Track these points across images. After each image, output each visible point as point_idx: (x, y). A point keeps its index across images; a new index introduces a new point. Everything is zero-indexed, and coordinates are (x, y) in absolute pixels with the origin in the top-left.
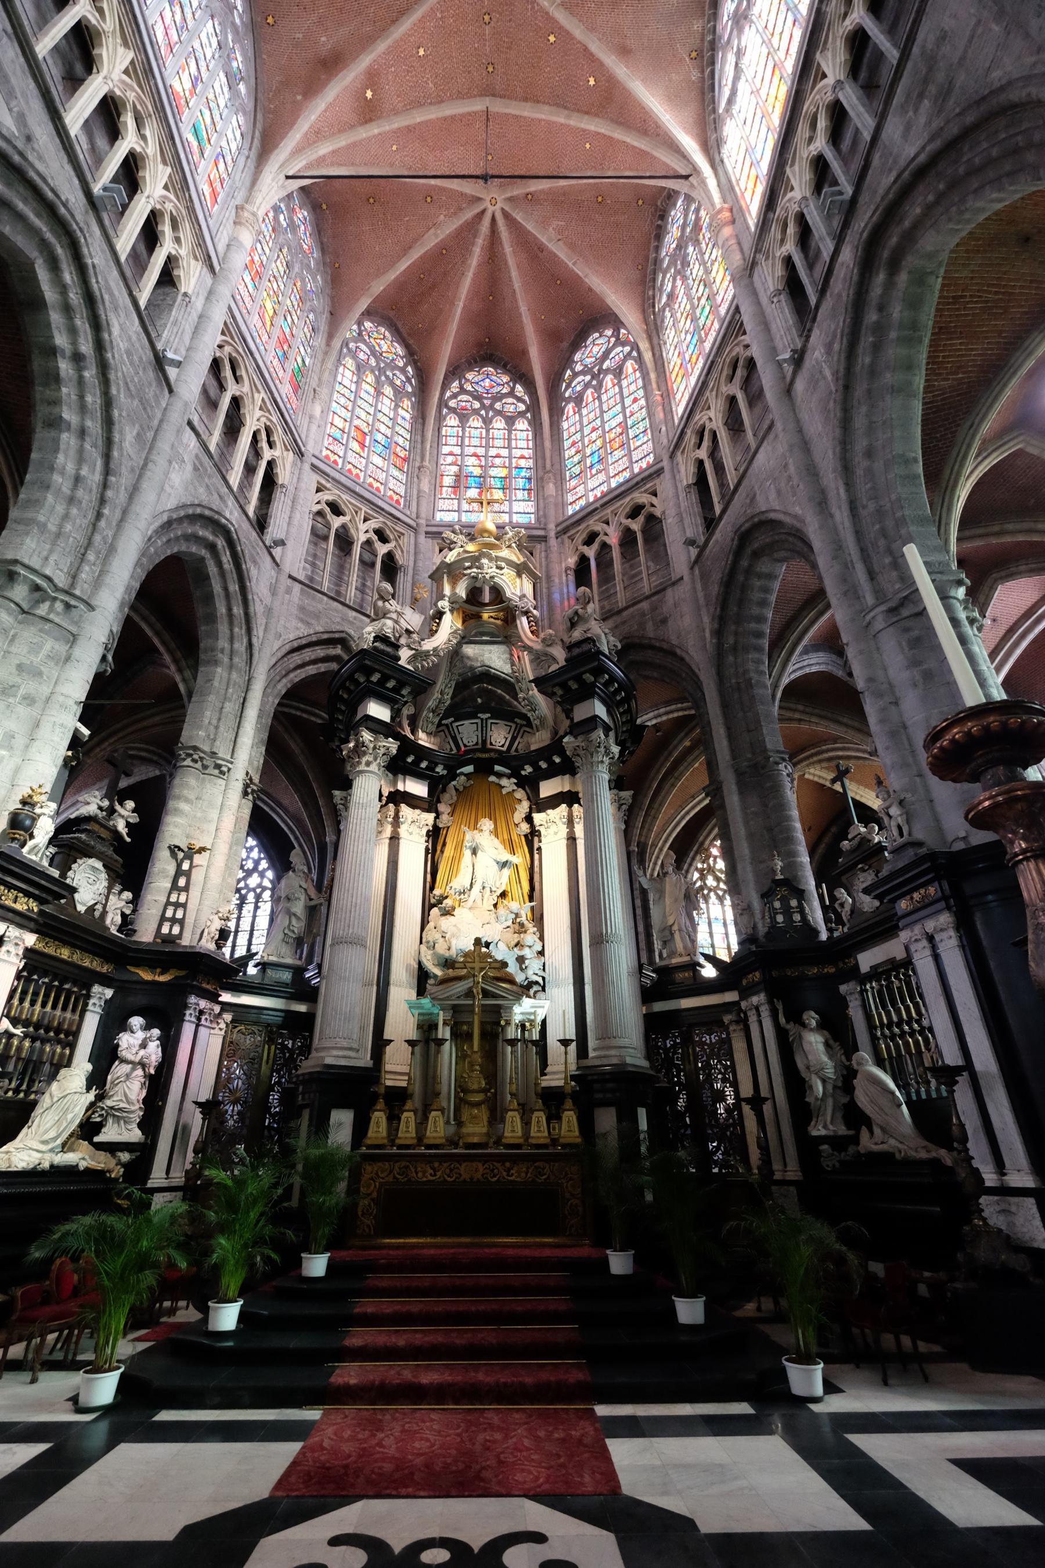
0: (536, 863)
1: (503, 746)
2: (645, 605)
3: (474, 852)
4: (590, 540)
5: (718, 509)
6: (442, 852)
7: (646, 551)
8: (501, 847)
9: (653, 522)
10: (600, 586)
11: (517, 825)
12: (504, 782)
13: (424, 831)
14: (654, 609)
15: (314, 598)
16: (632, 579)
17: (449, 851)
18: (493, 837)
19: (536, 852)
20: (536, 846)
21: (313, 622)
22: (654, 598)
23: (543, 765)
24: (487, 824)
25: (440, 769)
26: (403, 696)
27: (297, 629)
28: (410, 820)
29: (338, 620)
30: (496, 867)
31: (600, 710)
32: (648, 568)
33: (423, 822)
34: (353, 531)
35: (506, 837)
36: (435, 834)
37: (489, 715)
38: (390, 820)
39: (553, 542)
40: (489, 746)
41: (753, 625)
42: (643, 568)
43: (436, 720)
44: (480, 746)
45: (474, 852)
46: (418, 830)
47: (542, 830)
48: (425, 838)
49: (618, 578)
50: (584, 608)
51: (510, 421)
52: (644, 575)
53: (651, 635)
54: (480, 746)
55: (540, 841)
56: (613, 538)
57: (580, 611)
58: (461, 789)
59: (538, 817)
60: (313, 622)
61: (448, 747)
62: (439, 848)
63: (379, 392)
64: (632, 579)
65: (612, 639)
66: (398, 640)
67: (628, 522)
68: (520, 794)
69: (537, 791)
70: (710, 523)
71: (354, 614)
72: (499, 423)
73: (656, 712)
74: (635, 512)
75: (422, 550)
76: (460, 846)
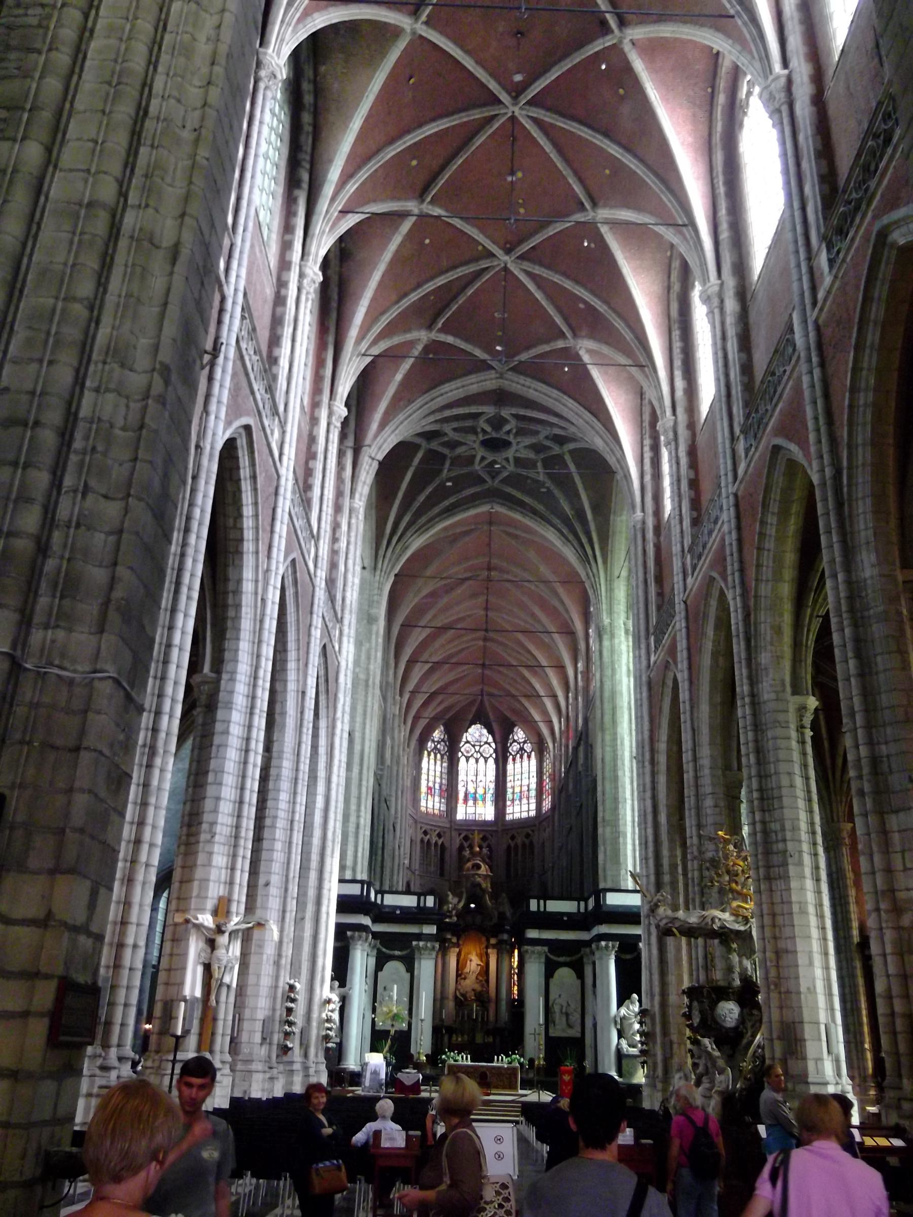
9: (531, 843)
36: (459, 955)
51: (486, 759)
72: (482, 760)
74: (528, 836)
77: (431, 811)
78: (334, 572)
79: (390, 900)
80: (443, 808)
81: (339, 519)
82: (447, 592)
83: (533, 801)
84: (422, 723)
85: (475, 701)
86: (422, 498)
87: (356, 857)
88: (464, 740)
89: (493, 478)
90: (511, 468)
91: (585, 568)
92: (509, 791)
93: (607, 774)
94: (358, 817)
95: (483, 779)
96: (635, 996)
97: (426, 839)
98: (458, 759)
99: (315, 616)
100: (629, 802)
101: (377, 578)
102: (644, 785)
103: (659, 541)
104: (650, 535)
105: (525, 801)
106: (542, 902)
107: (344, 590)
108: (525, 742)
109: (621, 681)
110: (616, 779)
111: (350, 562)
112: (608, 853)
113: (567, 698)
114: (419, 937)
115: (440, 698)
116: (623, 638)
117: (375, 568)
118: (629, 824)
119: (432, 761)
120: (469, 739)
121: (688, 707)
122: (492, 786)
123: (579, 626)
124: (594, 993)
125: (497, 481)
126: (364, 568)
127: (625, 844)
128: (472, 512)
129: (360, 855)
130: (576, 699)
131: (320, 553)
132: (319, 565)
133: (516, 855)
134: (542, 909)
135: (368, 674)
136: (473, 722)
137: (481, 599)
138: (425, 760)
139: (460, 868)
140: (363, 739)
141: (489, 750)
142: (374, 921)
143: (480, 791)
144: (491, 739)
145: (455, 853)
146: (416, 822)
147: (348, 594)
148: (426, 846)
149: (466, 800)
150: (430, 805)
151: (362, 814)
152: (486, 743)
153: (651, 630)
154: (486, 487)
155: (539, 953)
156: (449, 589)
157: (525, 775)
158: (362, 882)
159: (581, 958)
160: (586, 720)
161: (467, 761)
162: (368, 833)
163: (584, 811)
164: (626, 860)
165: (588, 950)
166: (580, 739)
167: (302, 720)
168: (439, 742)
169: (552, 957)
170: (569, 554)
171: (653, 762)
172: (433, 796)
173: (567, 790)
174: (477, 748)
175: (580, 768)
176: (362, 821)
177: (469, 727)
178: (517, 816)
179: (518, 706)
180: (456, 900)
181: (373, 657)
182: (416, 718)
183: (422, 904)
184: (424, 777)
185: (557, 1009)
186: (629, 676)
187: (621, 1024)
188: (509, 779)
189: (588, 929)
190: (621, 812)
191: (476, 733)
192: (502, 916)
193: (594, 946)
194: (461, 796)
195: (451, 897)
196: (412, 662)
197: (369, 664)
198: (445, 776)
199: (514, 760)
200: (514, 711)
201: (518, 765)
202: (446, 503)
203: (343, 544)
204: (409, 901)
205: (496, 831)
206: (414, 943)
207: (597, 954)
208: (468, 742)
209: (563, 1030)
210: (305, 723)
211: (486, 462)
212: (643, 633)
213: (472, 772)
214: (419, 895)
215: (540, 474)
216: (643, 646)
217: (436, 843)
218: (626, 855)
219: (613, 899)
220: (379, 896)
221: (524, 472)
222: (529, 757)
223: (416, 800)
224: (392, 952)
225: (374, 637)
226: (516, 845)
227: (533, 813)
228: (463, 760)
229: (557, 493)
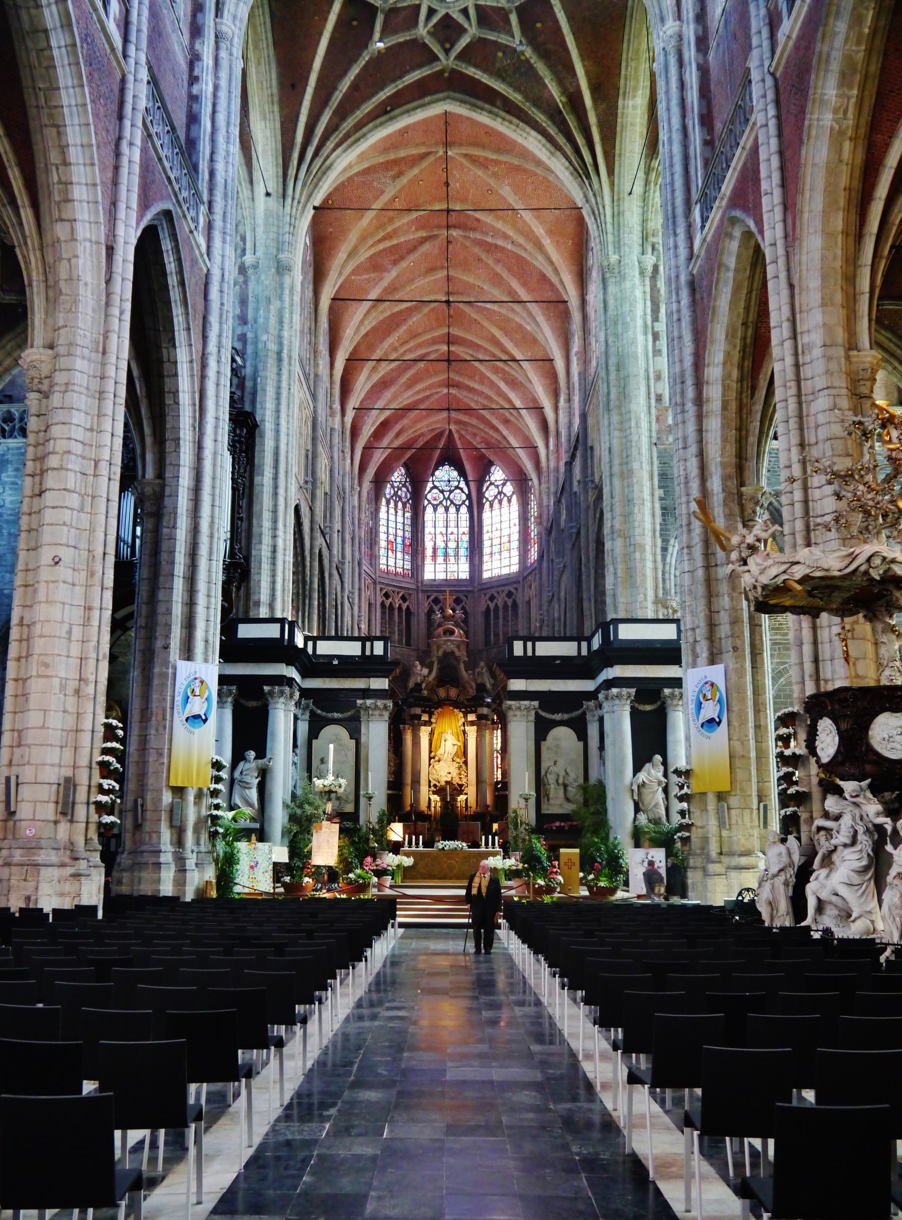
4: (492, 598)
9: (515, 604)
36: (432, 733)
56: (500, 605)
59: (467, 728)
68: (461, 715)
72: (452, 510)
77: (391, 569)
78: (194, 128)
79: (325, 648)
80: (408, 566)
81: (197, 46)
82: (395, 263)
83: (515, 553)
84: (378, 457)
85: (441, 434)
86: (345, 85)
87: (273, 590)
88: (430, 485)
89: (447, 52)
90: (473, 30)
91: (582, 186)
92: (486, 544)
93: (616, 469)
94: (275, 537)
95: (455, 531)
96: (658, 758)
97: (388, 603)
98: (424, 508)
99: (127, 123)
100: (648, 504)
101: (288, 208)
102: (685, 438)
103: (706, 61)
104: (691, 54)
105: (505, 554)
106: (529, 644)
107: (212, 160)
108: (504, 484)
109: (634, 342)
110: (627, 474)
111: (221, 117)
112: (620, 573)
113: (556, 409)
114: (366, 693)
115: (398, 427)
116: (637, 280)
117: (284, 196)
118: (649, 533)
119: (392, 511)
120: (436, 484)
121: (781, 251)
122: (466, 538)
123: (572, 294)
124: (602, 758)
125: (454, 54)
126: (268, 194)
127: (643, 560)
128: (420, 115)
129: (279, 586)
130: (569, 400)
131: (134, 17)
132: (133, 37)
133: (497, 617)
134: (530, 653)
135: (281, 344)
136: (440, 464)
137: (442, 274)
138: (383, 509)
139: (430, 635)
140: (277, 432)
141: (459, 497)
142: (304, 676)
143: (452, 545)
144: (463, 485)
145: (423, 617)
146: (375, 583)
147: (220, 166)
148: (387, 610)
149: (434, 556)
150: (391, 562)
151: (280, 533)
152: (457, 487)
153: (695, 196)
154: (437, 67)
155: (527, 709)
156: (398, 254)
157: (505, 525)
158: (282, 621)
159: (584, 713)
160: (584, 416)
161: (435, 510)
162: (290, 559)
163: (583, 533)
164: (644, 581)
165: (592, 704)
166: (576, 448)
167: (108, 295)
168: (399, 489)
169: (544, 714)
170: (559, 167)
171: (699, 401)
172: (395, 551)
173: (559, 525)
174: (447, 494)
175: (576, 488)
176: (280, 543)
177: (436, 468)
178: (496, 573)
179: (495, 435)
180: (425, 671)
181: (286, 320)
182: (368, 449)
183: (368, 653)
184: (382, 529)
185: (551, 779)
186: (646, 334)
187: (639, 794)
188: (485, 530)
189: (592, 676)
190: (638, 517)
191: (445, 474)
192: (481, 688)
193: (601, 696)
194: (429, 552)
195: (419, 667)
196: (354, 362)
197: (281, 330)
198: (408, 528)
199: (491, 506)
200: (490, 446)
201: (496, 512)
202: (382, 96)
203: (206, 87)
204: (352, 649)
205: (472, 592)
206: (359, 702)
207: (606, 705)
208: (435, 487)
209: (561, 805)
210: (116, 299)
211: (435, 19)
212: (680, 210)
213: (441, 524)
214: (363, 640)
215: (516, 40)
216: (681, 230)
217: (400, 608)
218: (644, 575)
219: (627, 632)
220: (310, 644)
221: (492, 36)
222: (509, 501)
223: (373, 558)
224: (330, 715)
225: (287, 292)
226: (496, 606)
227: (515, 568)
228: (429, 510)
229: (541, 68)
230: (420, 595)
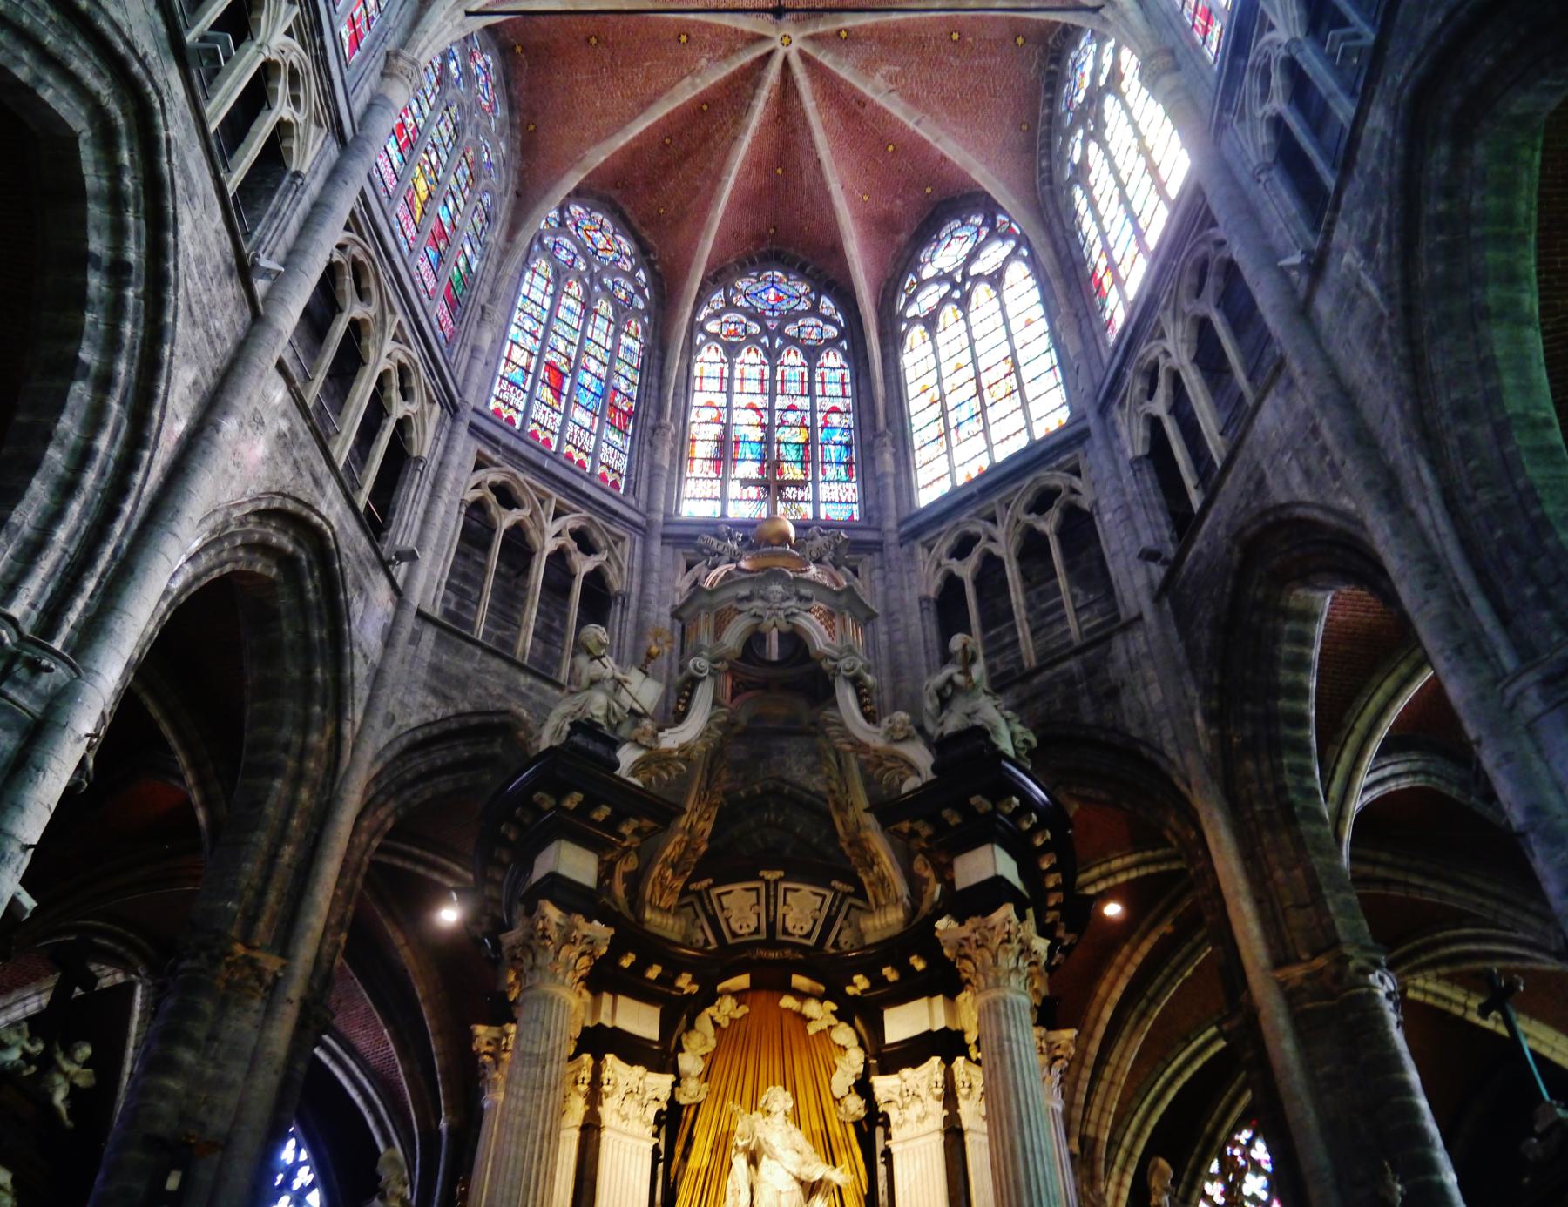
0: (882, 1185)
1: (808, 936)
2: (1073, 664)
3: (753, 1160)
4: (962, 548)
5: (1196, 499)
6: (685, 1157)
7: (1069, 568)
8: (808, 1148)
10: (985, 628)
11: (837, 1101)
12: (812, 1008)
13: (651, 1113)
14: (1090, 671)
15: (458, 650)
16: (1045, 616)
17: (700, 1156)
18: (791, 1126)
19: (879, 1160)
20: (880, 1147)
21: (455, 693)
22: (1090, 653)
23: (890, 974)
24: (778, 1099)
25: (685, 982)
26: (623, 837)
27: (424, 706)
28: (622, 1090)
29: (499, 690)
30: (798, 1194)
31: (1007, 867)
32: (1074, 598)
33: (650, 1095)
34: (534, 535)
35: (816, 1126)
37: (780, 874)
38: (583, 1088)
39: (893, 552)
40: (781, 937)
41: (1284, 704)
42: (1066, 597)
43: (679, 884)
44: (763, 936)
45: (753, 1160)
46: (639, 1111)
47: (894, 1116)
48: (651, 1129)
49: (1020, 614)
50: (966, 672)
51: (812, 354)
52: (1069, 610)
53: (1089, 718)
54: (763, 936)
55: (888, 1137)
56: (1005, 547)
57: (959, 679)
58: (725, 1023)
59: (883, 1085)
60: (455, 693)
61: (700, 936)
62: (679, 1149)
63: (588, 310)
64: (1045, 616)
65: (1018, 728)
66: (615, 729)
67: (1032, 518)
68: (844, 1035)
69: (877, 1028)
70: (1184, 522)
71: (530, 680)
73: (1104, 868)
75: (657, 565)
76: (722, 1144)
194: (704, 449)
226: (991, 566)
230: (656, 547)
